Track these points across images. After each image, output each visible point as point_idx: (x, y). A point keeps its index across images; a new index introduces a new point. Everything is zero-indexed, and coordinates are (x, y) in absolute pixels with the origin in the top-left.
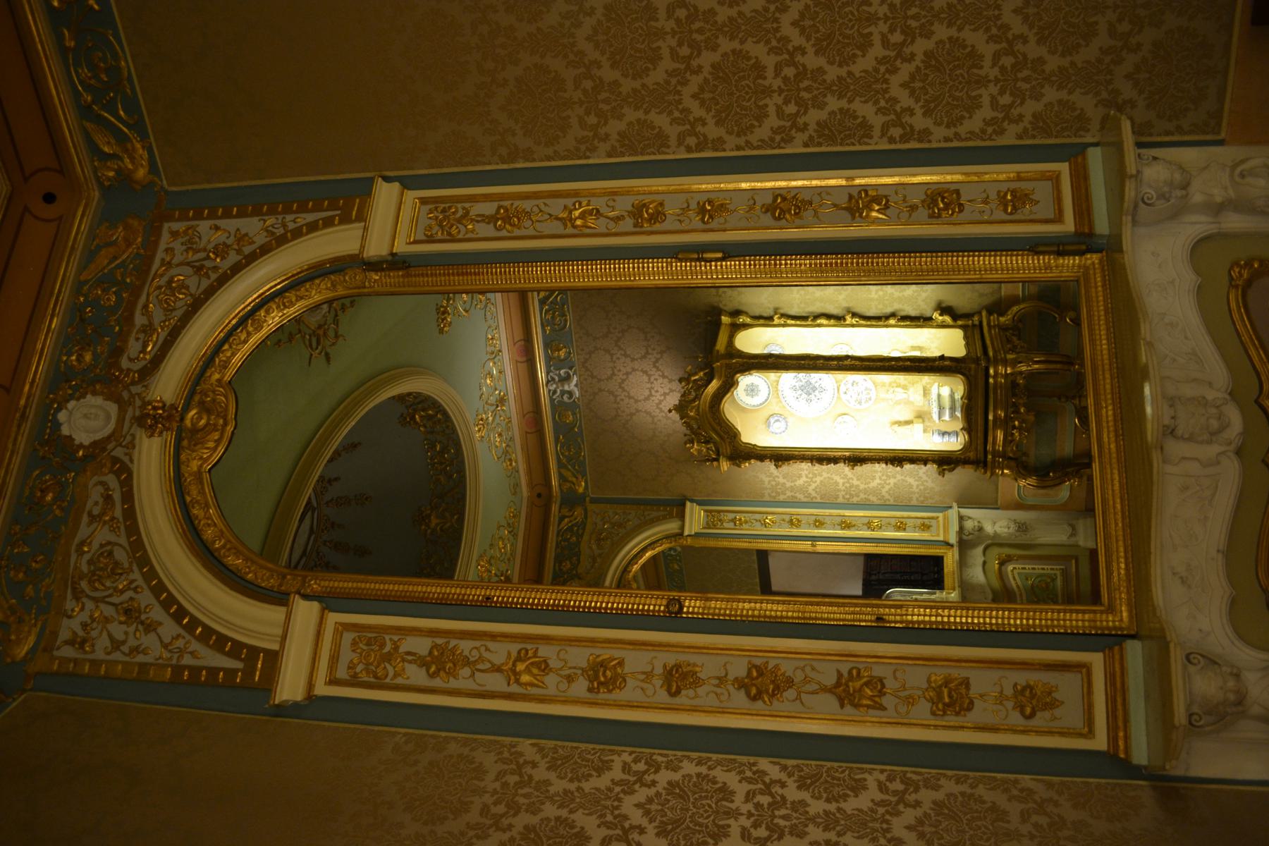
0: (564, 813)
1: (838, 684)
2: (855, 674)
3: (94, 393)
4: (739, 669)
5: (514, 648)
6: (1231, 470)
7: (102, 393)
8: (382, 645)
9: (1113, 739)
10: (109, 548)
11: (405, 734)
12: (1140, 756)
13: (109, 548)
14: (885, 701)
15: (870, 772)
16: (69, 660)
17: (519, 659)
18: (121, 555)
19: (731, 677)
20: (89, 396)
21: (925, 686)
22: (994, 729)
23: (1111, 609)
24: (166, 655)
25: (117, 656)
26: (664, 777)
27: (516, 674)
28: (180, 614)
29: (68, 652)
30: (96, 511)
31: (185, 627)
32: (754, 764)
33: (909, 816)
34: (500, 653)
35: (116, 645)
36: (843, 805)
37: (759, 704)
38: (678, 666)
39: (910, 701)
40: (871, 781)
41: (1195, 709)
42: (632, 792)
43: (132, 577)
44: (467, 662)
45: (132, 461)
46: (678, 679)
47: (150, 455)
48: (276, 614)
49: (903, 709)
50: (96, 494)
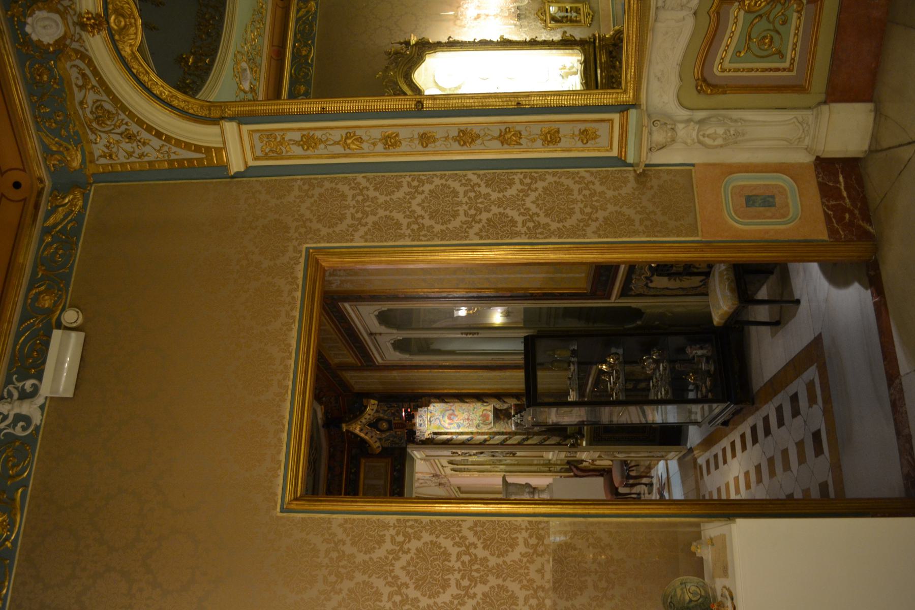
0: (387, 213)
1: (500, 135)
2: (508, 130)
3: (39, 9)
4: (454, 133)
5: (344, 132)
6: (690, 22)
7: (44, 9)
8: (275, 138)
9: (620, 152)
10: (99, 103)
11: (302, 179)
12: (630, 159)
13: (99, 103)
14: (522, 141)
15: (516, 174)
16: (107, 165)
17: (347, 138)
18: (108, 106)
19: (451, 136)
20: (37, 12)
21: (539, 133)
22: (569, 150)
23: (625, 92)
24: (160, 156)
25: (132, 159)
26: (427, 188)
27: (348, 145)
28: (159, 135)
29: (103, 161)
30: (80, 83)
31: (164, 141)
32: (465, 176)
33: (533, 196)
34: (337, 136)
35: (130, 154)
36: (505, 194)
37: (465, 147)
38: (425, 134)
39: (533, 141)
40: (517, 178)
41: (654, 145)
42: (415, 198)
43: (120, 117)
44: (321, 141)
45: (87, 50)
46: (425, 139)
47: (97, 45)
48: (214, 129)
49: (530, 144)
50: (74, 74)
